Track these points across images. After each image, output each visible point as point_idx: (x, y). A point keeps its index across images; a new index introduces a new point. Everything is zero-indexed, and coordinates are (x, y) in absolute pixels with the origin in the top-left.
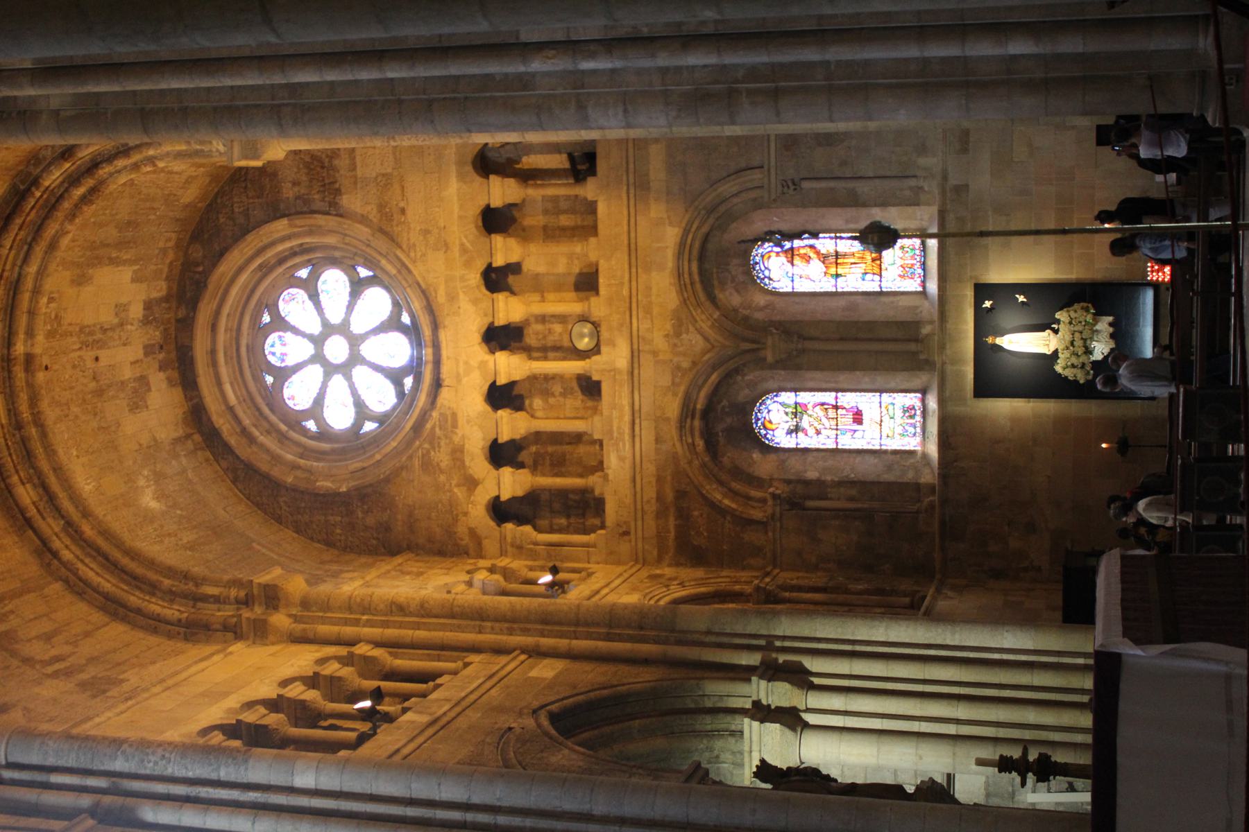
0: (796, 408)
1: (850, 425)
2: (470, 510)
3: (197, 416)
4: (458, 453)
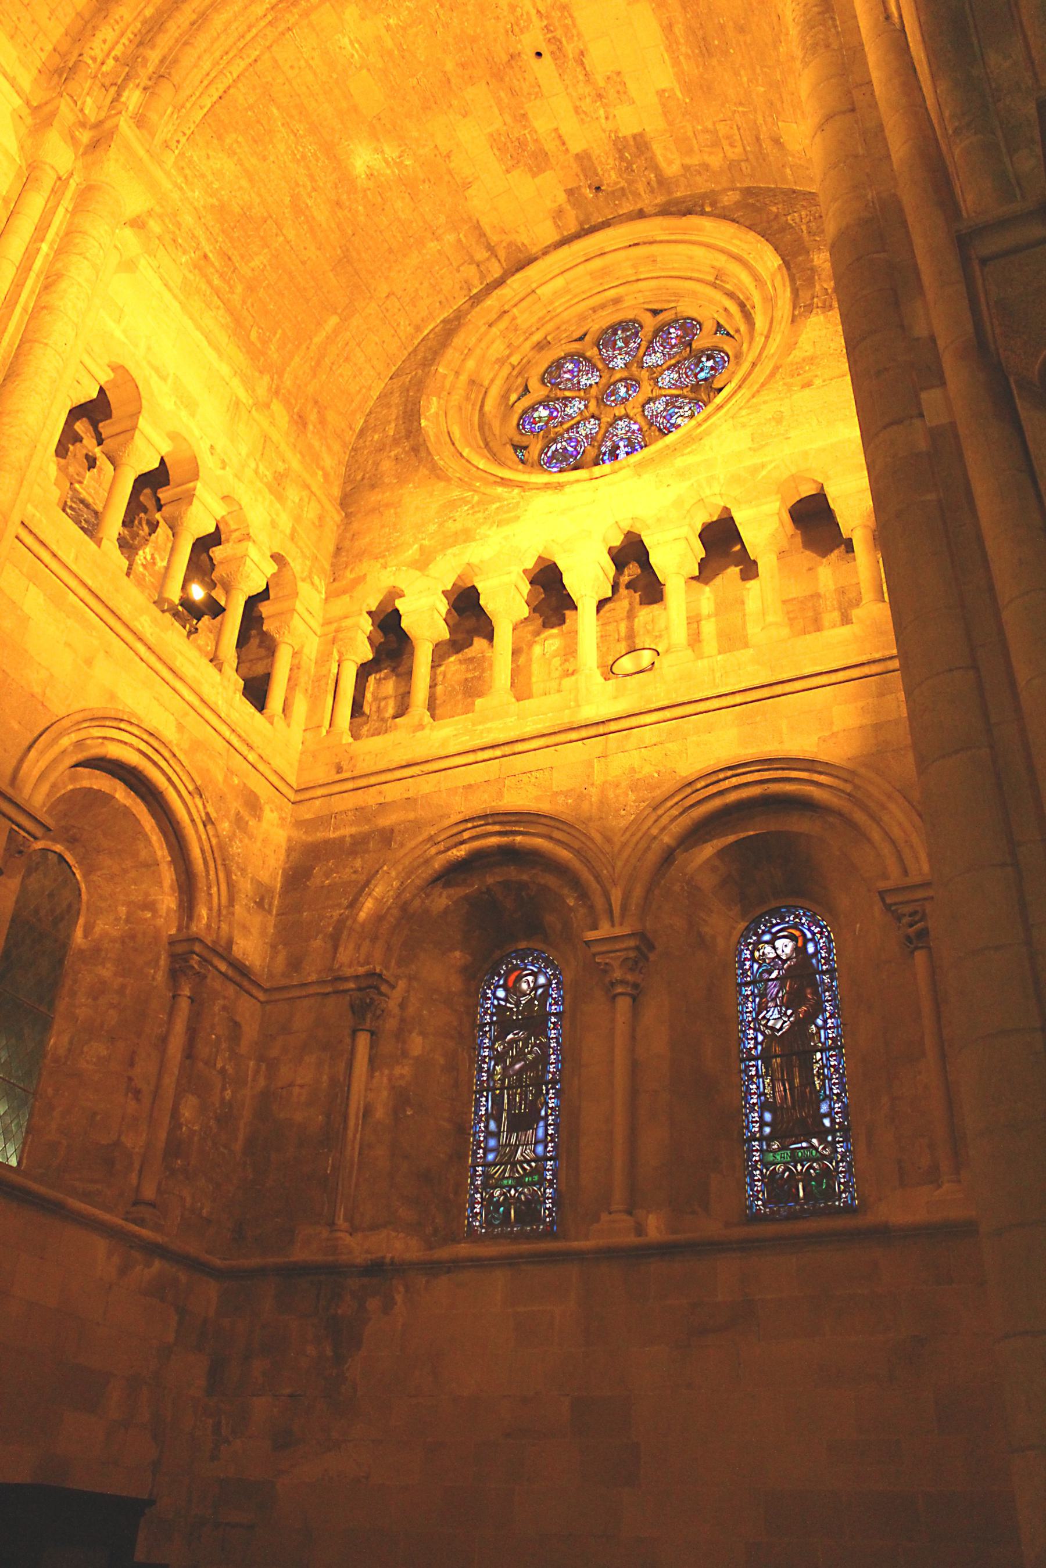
1: (509, 1111)
2: (389, 569)
4: (466, 536)
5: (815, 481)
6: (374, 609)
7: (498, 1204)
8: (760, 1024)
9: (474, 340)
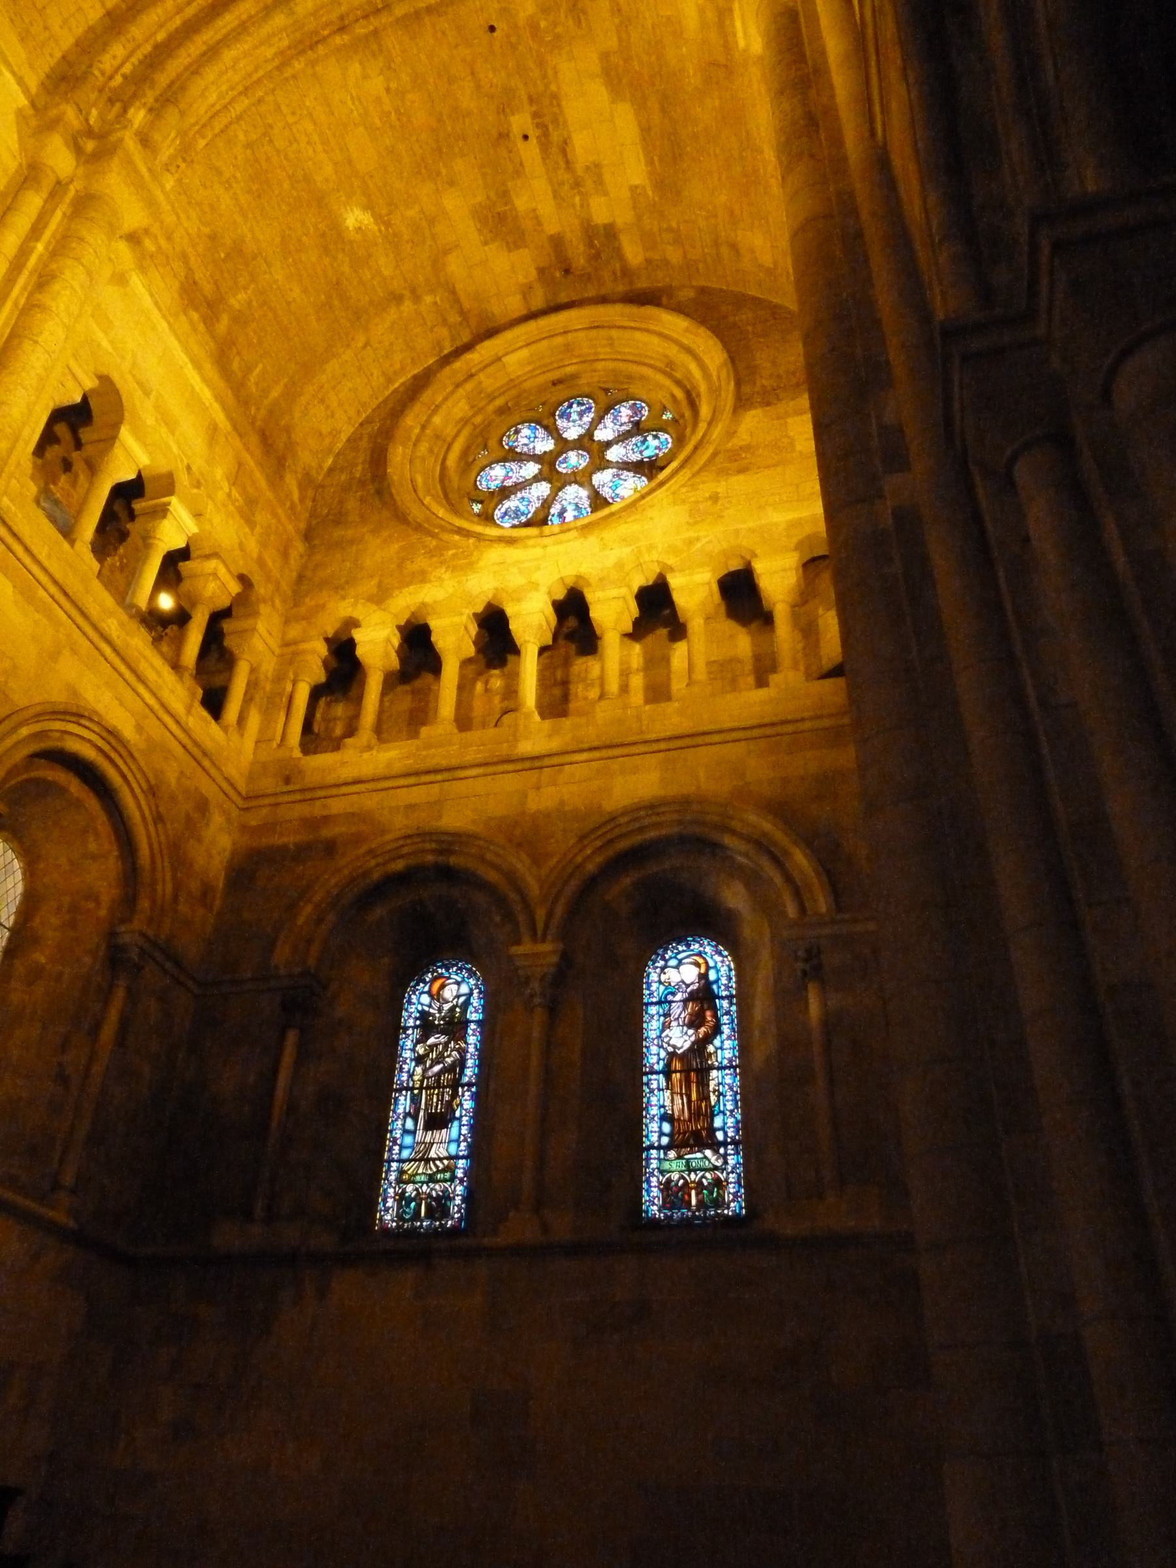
0: (460, 1022)
1: (426, 1109)
2: (347, 601)
4: (422, 577)
5: (742, 557)
6: (330, 636)
8: (663, 1041)
9: (440, 399)
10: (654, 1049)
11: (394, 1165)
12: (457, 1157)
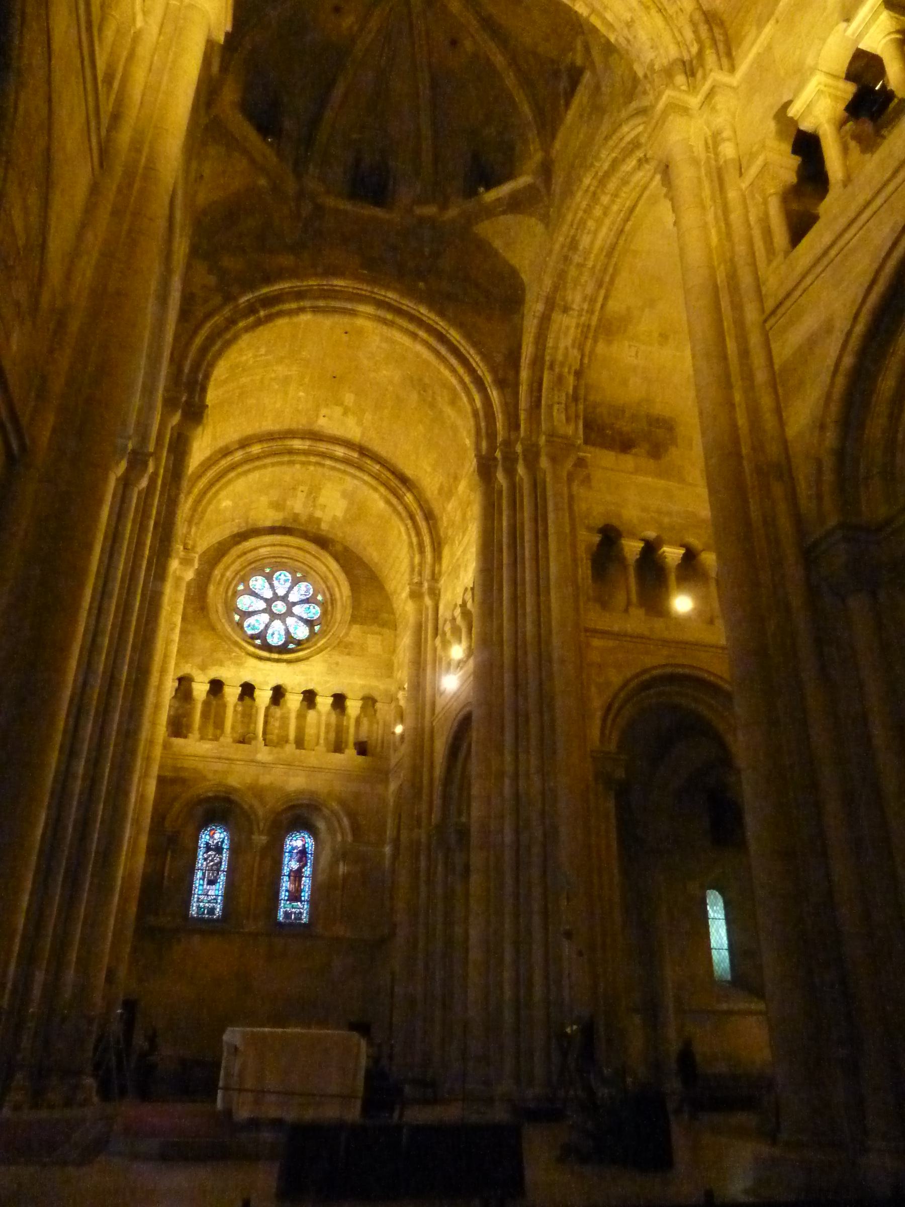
1: (208, 878)
3: (256, 532)
4: (221, 664)
7: (201, 908)
10: (286, 868)
11: (196, 896)
12: (218, 896)
